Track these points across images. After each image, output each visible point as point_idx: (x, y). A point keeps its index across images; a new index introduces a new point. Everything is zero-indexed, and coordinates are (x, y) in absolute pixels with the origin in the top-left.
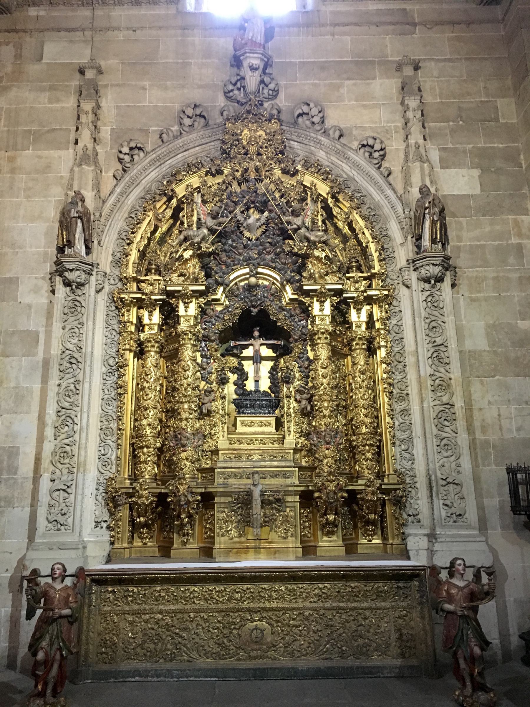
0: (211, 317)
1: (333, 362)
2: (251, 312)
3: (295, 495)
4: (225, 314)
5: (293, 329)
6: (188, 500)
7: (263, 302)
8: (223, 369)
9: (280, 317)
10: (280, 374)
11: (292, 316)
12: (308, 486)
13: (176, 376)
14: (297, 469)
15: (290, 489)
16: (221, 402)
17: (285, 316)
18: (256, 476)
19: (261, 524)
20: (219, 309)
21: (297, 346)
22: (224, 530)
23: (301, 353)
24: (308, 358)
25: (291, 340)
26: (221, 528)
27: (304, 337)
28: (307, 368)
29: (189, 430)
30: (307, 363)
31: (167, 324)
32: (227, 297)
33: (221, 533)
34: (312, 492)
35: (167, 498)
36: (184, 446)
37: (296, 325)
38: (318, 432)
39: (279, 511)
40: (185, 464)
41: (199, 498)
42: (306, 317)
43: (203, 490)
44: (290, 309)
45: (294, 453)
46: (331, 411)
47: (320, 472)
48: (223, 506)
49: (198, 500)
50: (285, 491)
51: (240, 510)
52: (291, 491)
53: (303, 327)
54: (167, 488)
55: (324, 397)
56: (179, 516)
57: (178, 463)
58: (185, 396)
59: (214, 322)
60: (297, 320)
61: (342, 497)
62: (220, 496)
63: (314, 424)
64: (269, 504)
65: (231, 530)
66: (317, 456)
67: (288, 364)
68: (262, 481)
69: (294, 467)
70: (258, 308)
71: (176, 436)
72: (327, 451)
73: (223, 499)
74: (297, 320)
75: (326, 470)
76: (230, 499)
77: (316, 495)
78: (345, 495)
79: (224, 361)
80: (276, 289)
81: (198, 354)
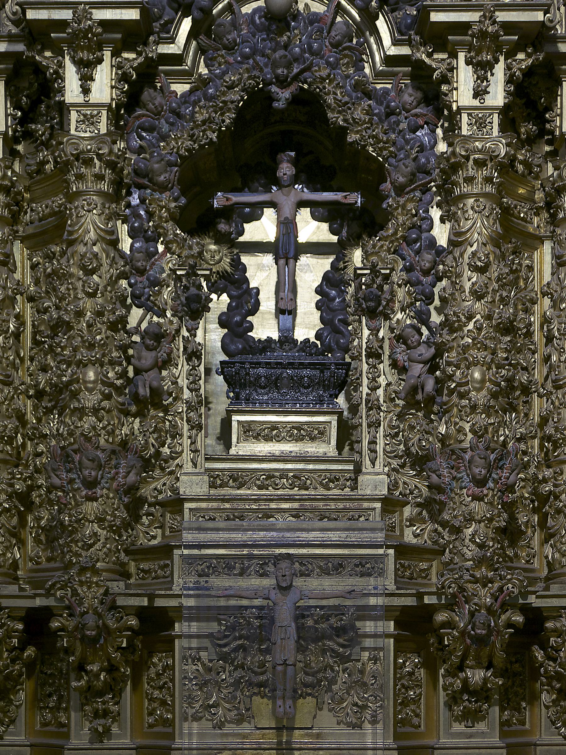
0: (158, 114)
1: (503, 257)
2: (270, 98)
3: (388, 619)
4: (195, 104)
5: (393, 155)
6: (105, 625)
7: (308, 69)
8: (192, 272)
9: (358, 114)
10: (351, 290)
11: (390, 113)
12: (420, 596)
13: (63, 289)
14: (391, 551)
15: (373, 601)
16: (186, 367)
17: (369, 112)
18: (284, 565)
19: (295, 691)
20: (180, 88)
21: (404, 207)
22: (197, 706)
23: (414, 226)
24: (433, 241)
25: (387, 186)
26: (190, 699)
27: (422, 179)
28: (426, 273)
29: (102, 442)
30: (428, 257)
31: (28, 135)
32: (202, 50)
33: (191, 712)
34: (432, 610)
35: (48, 620)
36: (91, 484)
37: (400, 140)
38: (453, 451)
39: (344, 659)
40: (95, 534)
41: (133, 622)
42: (431, 116)
43: (145, 602)
44: (386, 92)
45: (384, 511)
46: (494, 396)
47: (451, 560)
48: (194, 643)
49: (130, 628)
50: (359, 608)
51: (241, 655)
52: (375, 607)
53: (422, 148)
54: (48, 594)
55: (474, 352)
56: (81, 668)
57: (74, 531)
58: (91, 346)
59: (165, 128)
60: (403, 125)
61: (510, 625)
62: (190, 619)
63: (443, 429)
64: (316, 640)
65: (214, 706)
66: (446, 516)
67: (374, 259)
68: (298, 582)
69: (388, 547)
70: (293, 88)
71: (67, 458)
72: (476, 506)
73: (195, 627)
74: (403, 125)
75: (469, 554)
76: (214, 627)
77: (441, 617)
78: (519, 619)
79: (196, 250)
80: (346, 23)
81: (123, 229)
